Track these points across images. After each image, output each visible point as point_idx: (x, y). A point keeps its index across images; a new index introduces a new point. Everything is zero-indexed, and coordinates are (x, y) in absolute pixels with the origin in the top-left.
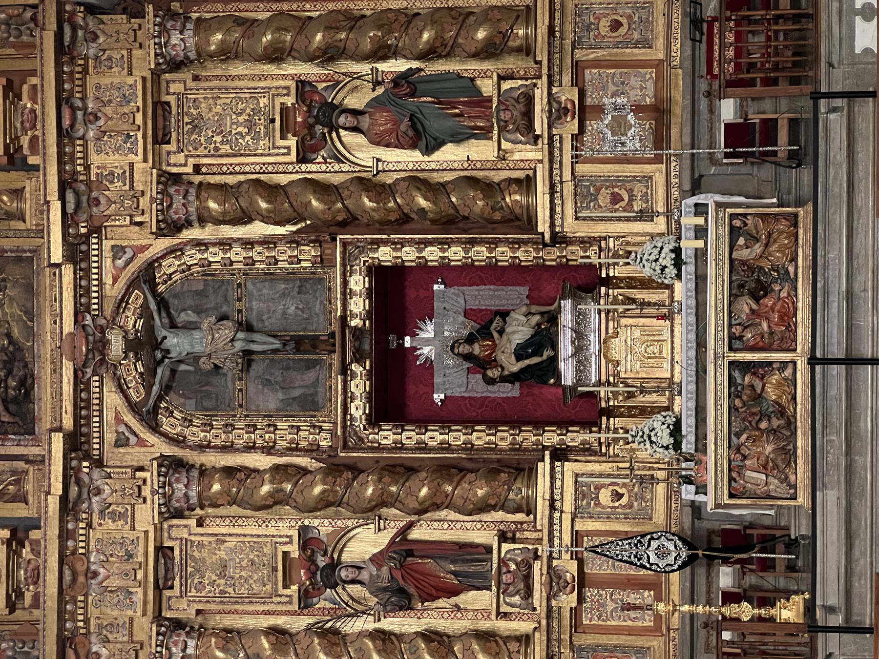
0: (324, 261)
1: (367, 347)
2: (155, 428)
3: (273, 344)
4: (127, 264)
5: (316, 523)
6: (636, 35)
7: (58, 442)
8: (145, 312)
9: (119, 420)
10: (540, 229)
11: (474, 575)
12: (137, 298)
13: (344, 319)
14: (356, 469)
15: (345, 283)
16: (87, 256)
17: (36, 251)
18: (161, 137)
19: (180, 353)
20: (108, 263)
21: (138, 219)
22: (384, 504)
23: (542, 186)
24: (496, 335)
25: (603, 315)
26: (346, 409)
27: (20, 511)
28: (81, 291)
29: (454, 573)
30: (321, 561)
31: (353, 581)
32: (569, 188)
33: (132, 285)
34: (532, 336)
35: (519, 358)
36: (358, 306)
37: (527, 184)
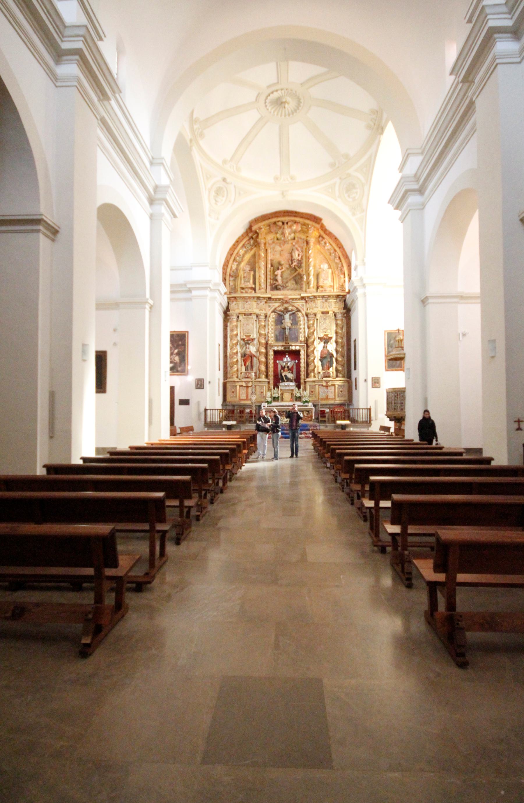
0: (301, 342)
2: (272, 312)
5: (256, 341)
6: (340, 395)
7: (269, 296)
8: (292, 310)
9: (273, 306)
11: (248, 368)
12: (294, 309)
13: (291, 345)
14: (266, 348)
15: (297, 346)
16: (302, 300)
17: (303, 291)
18: (323, 313)
20: (301, 303)
21: (308, 309)
22: (260, 353)
23: (314, 379)
26: (276, 346)
27: (257, 288)
28: (296, 299)
29: (248, 365)
30: (249, 342)
31: (246, 348)
32: (314, 384)
33: (297, 308)
36: (293, 348)
37: (315, 377)
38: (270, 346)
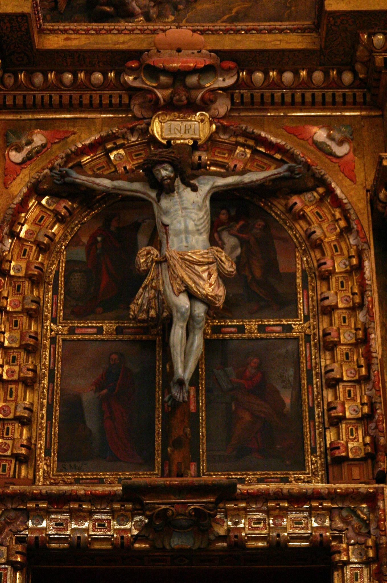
3: (186, 354)
4: (320, 147)
19: (166, 213)
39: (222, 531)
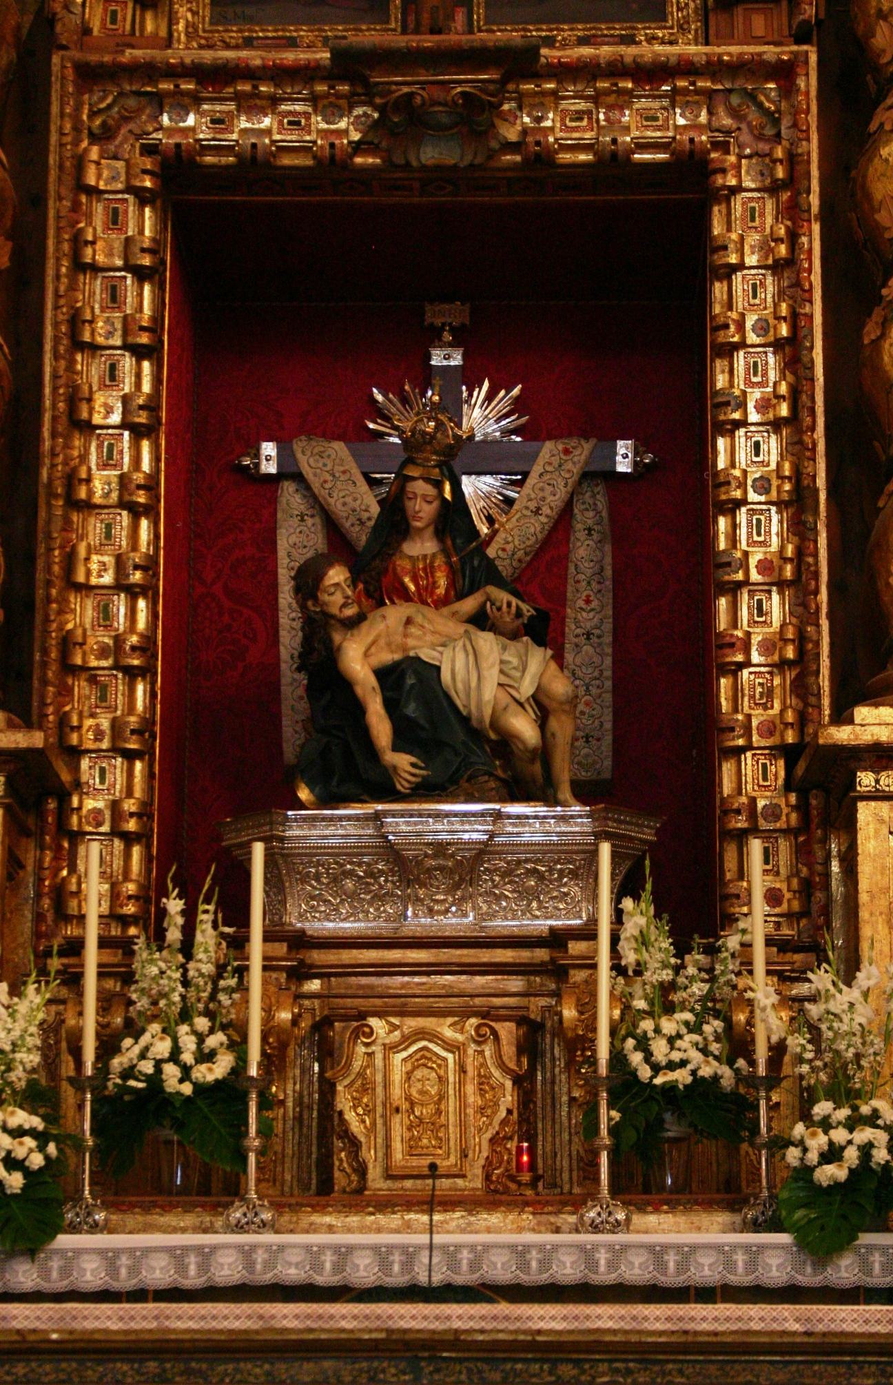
1: (430, 154)
10: (863, 713)
24: (469, 605)
25: (542, 954)
34: (465, 720)
35: (387, 676)
38: (89, 76)
39: (512, 134)
